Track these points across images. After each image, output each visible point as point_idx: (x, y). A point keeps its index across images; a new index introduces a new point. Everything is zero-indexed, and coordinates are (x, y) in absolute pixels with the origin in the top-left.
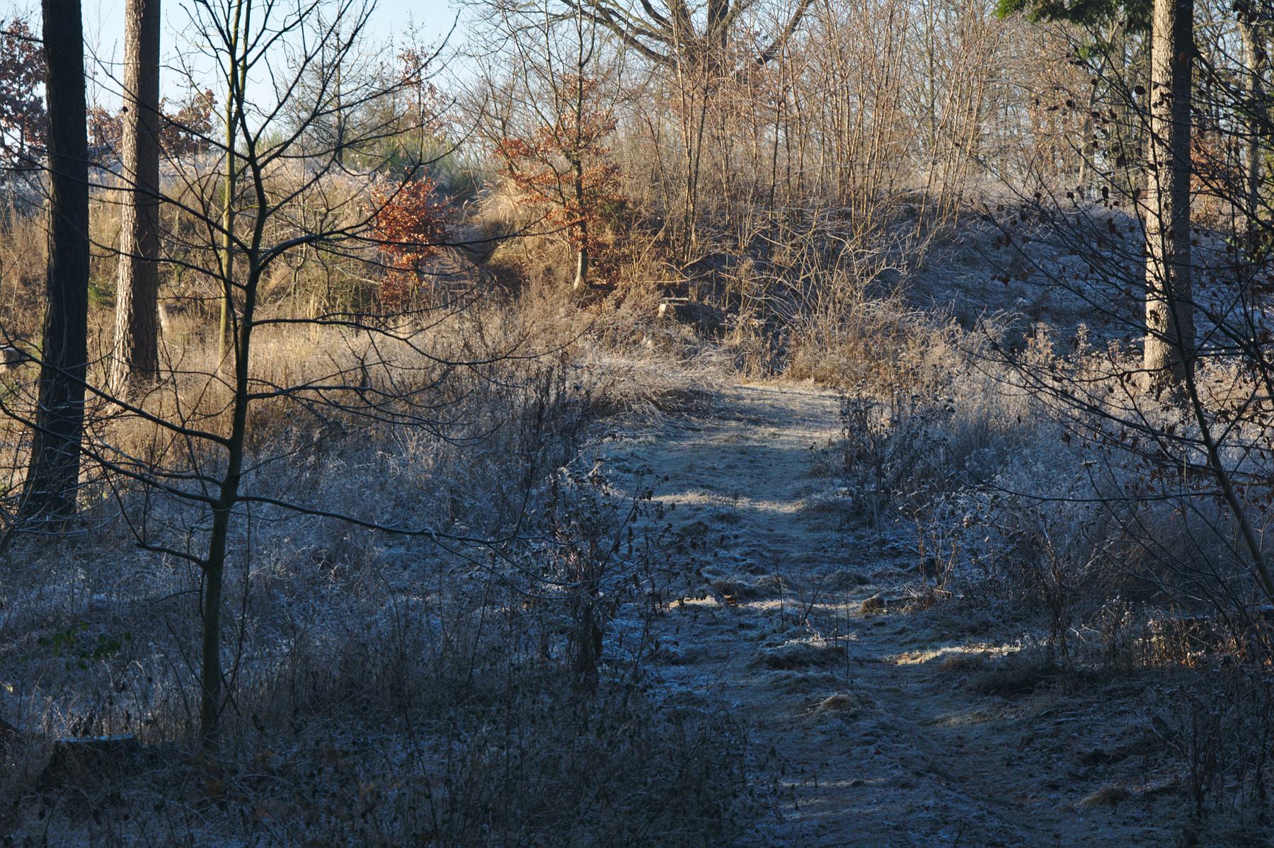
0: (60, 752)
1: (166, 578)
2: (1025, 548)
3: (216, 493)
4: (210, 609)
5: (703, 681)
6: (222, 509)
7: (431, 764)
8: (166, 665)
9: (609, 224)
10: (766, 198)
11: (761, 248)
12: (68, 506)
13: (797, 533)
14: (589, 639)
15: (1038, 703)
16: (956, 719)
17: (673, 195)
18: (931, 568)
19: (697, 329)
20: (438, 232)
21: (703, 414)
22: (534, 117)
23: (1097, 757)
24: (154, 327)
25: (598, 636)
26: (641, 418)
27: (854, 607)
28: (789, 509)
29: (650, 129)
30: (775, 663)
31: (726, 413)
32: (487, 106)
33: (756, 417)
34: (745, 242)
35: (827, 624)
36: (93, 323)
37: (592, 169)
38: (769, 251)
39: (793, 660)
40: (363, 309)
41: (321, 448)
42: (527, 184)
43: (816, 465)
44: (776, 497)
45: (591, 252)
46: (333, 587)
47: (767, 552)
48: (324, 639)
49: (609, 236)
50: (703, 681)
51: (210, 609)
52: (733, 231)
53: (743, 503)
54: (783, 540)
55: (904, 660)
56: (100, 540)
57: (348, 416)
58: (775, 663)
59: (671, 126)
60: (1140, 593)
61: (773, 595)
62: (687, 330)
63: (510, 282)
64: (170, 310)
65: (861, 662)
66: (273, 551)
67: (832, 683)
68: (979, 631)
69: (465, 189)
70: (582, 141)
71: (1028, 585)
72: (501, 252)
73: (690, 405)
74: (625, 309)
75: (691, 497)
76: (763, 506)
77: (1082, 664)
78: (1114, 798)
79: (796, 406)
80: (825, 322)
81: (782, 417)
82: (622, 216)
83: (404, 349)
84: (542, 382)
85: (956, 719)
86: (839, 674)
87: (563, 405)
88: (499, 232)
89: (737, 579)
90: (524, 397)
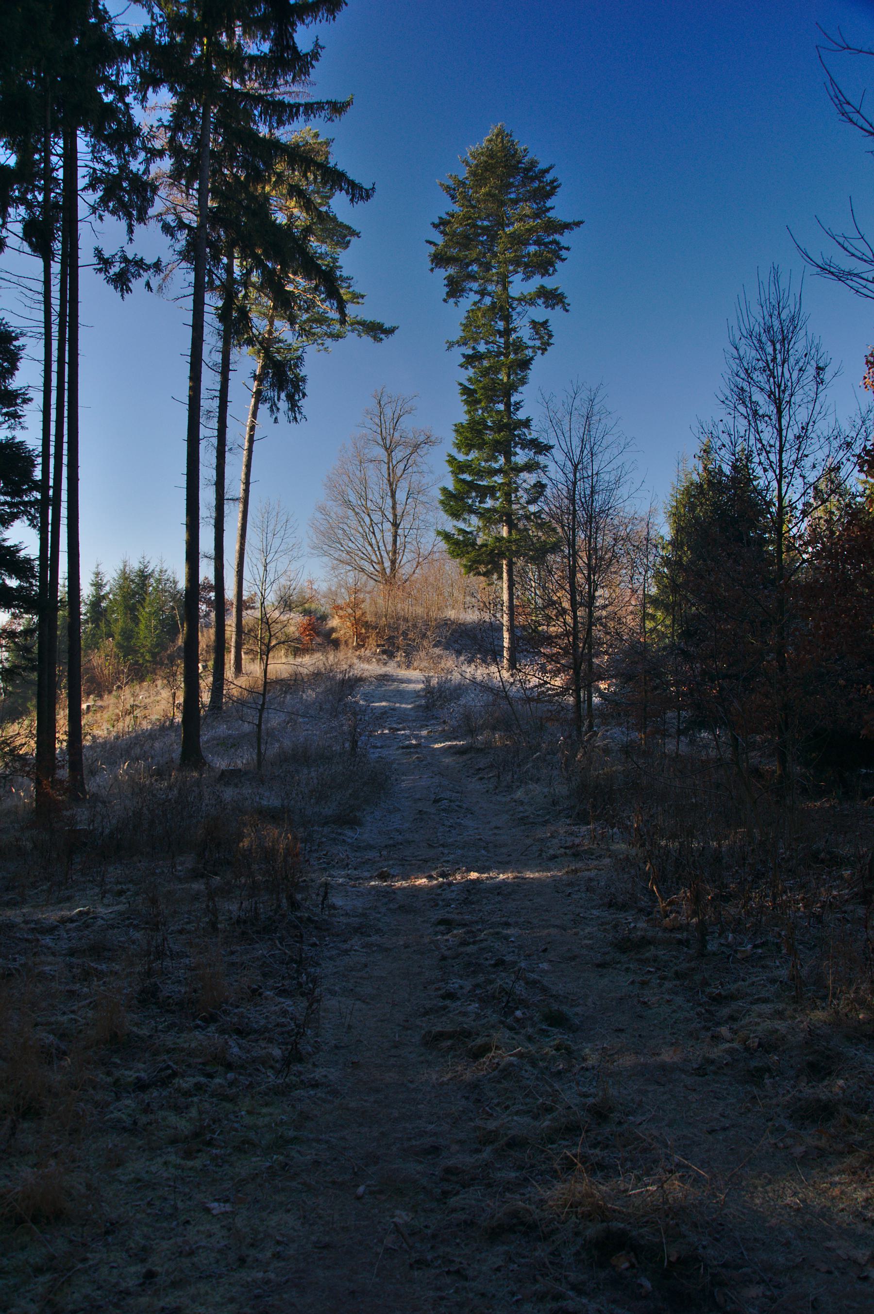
0: (223, 772)
1: (246, 728)
2: (467, 717)
3: (259, 707)
4: (259, 737)
5: (385, 752)
6: (261, 711)
7: (313, 774)
8: (248, 750)
9: (364, 629)
10: (406, 620)
11: (405, 634)
12: (220, 708)
13: (412, 713)
14: (354, 743)
15: (465, 757)
16: (447, 760)
17: (381, 619)
18: (444, 722)
19: (388, 656)
20: (318, 634)
21: (388, 681)
22: (344, 598)
23: (479, 769)
24: (241, 659)
25: (357, 742)
26: (371, 682)
27: (424, 733)
28: (410, 706)
29: (376, 602)
30: (403, 748)
31: (394, 680)
32: (332, 595)
33: (402, 681)
34: (401, 632)
35: (416, 737)
36: (226, 657)
37: (359, 613)
38: (407, 634)
39: (408, 747)
40: (297, 651)
41: (286, 692)
42: (341, 617)
43: (416, 694)
44: (406, 703)
45: (359, 635)
46: (289, 729)
47: (403, 718)
48: (287, 743)
49: (363, 631)
50: (385, 752)
51: (259, 737)
52: (397, 629)
53: (398, 705)
54: (408, 715)
55: (436, 746)
56: (230, 717)
57: (292, 684)
58: (403, 748)
59: (380, 601)
60: (494, 729)
61: (404, 730)
62: (385, 657)
63: (336, 644)
64: (245, 653)
65: (425, 747)
66: (274, 720)
67: (417, 753)
68: (455, 739)
69: (324, 618)
70: (356, 605)
71: (468, 726)
72: (334, 635)
73: (384, 678)
74: (368, 651)
75: (384, 704)
76: (403, 706)
77: (479, 746)
78: (481, 779)
79: (413, 678)
80: (422, 654)
81: (409, 681)
82: (367, 625)
83: (308, 663)
84: (344, 672)
85: (447, 760)
86: (419, 750)
87: (349, 679)
88: (333, 630)
89: (395, 726)
90: (339, 676)
